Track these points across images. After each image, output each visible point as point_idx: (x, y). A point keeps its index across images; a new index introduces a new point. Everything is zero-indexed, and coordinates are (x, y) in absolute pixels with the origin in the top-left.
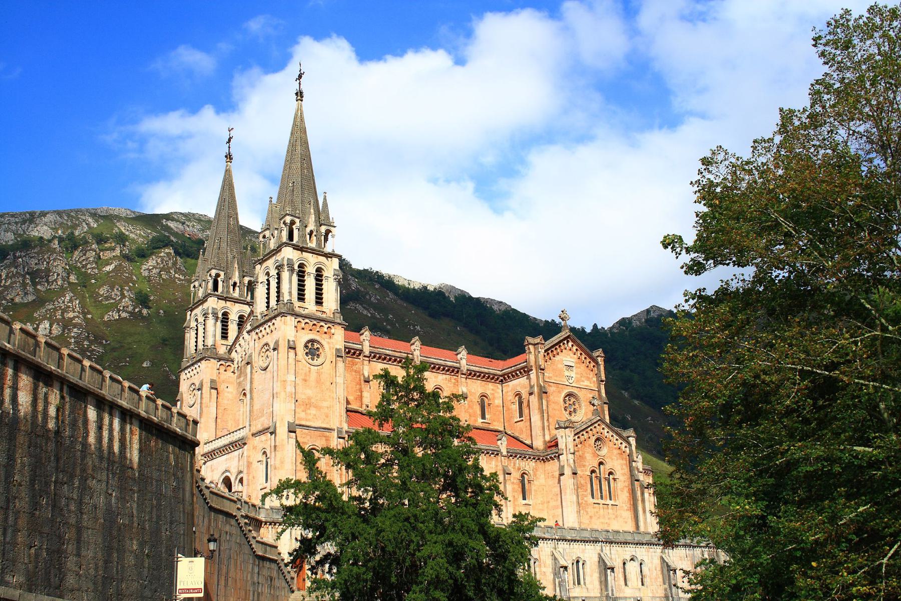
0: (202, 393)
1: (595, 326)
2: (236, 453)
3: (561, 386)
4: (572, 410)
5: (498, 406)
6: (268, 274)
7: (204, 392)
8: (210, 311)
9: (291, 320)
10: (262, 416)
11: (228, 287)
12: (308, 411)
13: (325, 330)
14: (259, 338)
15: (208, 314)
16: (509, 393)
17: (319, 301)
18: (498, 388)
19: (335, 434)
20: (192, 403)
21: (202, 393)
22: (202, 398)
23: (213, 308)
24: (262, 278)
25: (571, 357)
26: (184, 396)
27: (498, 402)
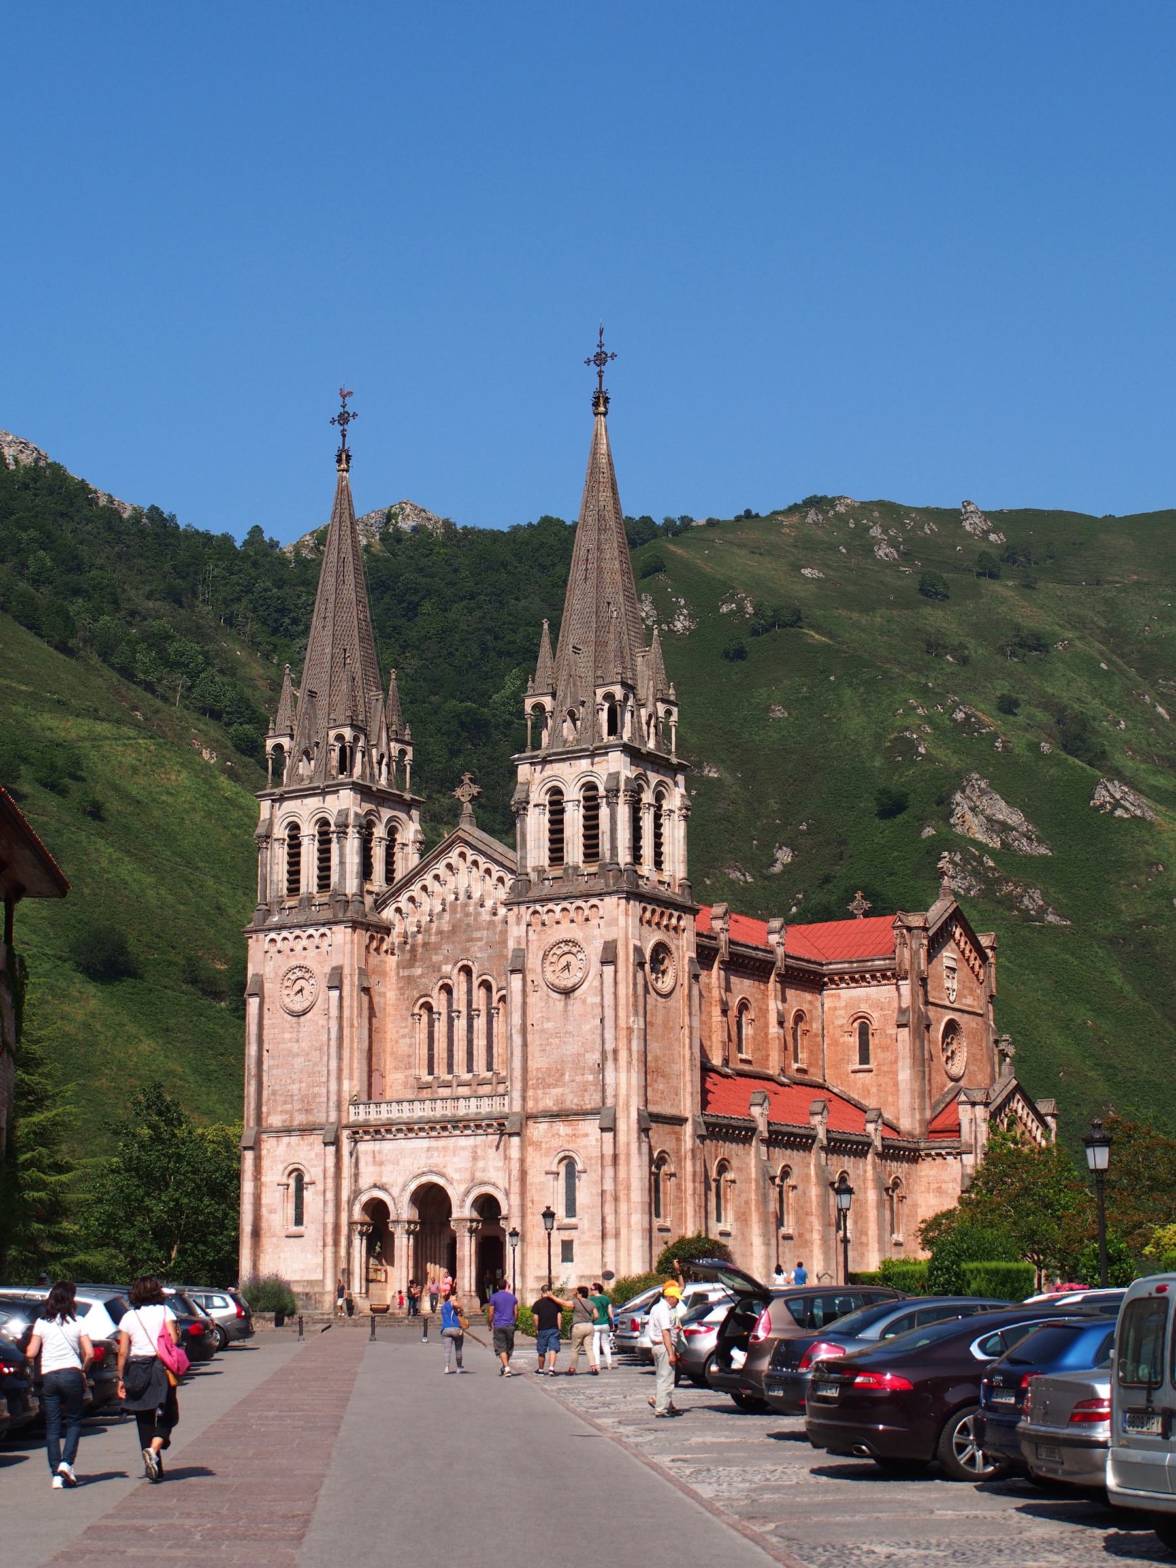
0: (341, 998)
1: (257, 531)
2: (463, 1142)
3: (939, 1009)
4: (949, 1054)
5: (816, 1035)
6: (556, 792)
7: (346, 993)
8: (351, 819)
9: (635, 907)
10: (559, 1082)
11: (372, 768)
12: (656, 1086)
13: (674, 921)
14: (544, 924)
15: (347, 826)
16: (839, 1012)
17: (658, 864)
18: (817, 999)
19: (688, 1128)
20: (298, 1007)
21: (341, 998)
22: (341, 1007)
23: (357, 815)
24: (539, 795)
25: (953, 951)
26: (266, 986)
27: (816, 1026)
